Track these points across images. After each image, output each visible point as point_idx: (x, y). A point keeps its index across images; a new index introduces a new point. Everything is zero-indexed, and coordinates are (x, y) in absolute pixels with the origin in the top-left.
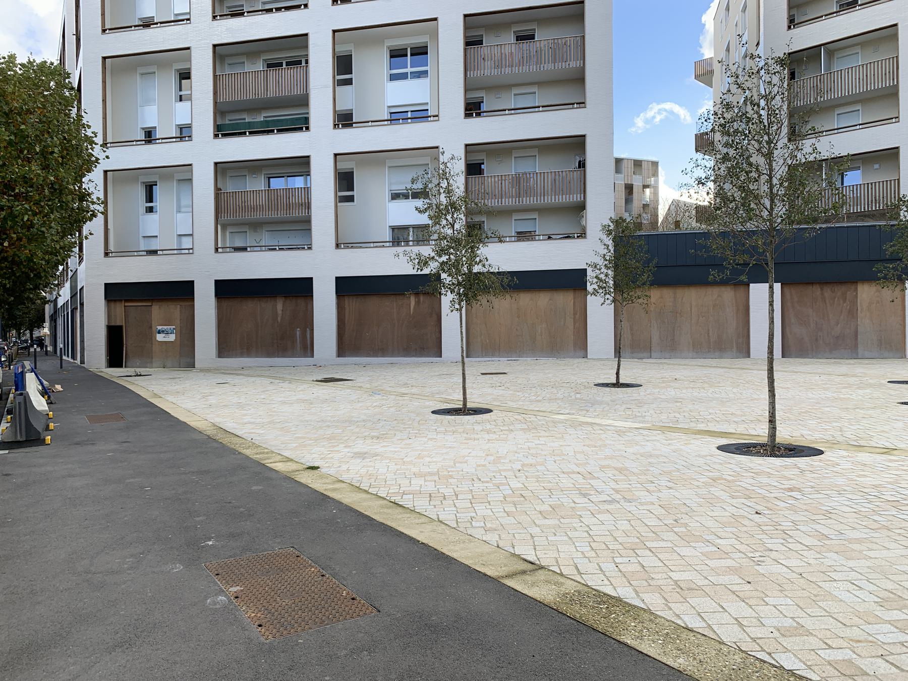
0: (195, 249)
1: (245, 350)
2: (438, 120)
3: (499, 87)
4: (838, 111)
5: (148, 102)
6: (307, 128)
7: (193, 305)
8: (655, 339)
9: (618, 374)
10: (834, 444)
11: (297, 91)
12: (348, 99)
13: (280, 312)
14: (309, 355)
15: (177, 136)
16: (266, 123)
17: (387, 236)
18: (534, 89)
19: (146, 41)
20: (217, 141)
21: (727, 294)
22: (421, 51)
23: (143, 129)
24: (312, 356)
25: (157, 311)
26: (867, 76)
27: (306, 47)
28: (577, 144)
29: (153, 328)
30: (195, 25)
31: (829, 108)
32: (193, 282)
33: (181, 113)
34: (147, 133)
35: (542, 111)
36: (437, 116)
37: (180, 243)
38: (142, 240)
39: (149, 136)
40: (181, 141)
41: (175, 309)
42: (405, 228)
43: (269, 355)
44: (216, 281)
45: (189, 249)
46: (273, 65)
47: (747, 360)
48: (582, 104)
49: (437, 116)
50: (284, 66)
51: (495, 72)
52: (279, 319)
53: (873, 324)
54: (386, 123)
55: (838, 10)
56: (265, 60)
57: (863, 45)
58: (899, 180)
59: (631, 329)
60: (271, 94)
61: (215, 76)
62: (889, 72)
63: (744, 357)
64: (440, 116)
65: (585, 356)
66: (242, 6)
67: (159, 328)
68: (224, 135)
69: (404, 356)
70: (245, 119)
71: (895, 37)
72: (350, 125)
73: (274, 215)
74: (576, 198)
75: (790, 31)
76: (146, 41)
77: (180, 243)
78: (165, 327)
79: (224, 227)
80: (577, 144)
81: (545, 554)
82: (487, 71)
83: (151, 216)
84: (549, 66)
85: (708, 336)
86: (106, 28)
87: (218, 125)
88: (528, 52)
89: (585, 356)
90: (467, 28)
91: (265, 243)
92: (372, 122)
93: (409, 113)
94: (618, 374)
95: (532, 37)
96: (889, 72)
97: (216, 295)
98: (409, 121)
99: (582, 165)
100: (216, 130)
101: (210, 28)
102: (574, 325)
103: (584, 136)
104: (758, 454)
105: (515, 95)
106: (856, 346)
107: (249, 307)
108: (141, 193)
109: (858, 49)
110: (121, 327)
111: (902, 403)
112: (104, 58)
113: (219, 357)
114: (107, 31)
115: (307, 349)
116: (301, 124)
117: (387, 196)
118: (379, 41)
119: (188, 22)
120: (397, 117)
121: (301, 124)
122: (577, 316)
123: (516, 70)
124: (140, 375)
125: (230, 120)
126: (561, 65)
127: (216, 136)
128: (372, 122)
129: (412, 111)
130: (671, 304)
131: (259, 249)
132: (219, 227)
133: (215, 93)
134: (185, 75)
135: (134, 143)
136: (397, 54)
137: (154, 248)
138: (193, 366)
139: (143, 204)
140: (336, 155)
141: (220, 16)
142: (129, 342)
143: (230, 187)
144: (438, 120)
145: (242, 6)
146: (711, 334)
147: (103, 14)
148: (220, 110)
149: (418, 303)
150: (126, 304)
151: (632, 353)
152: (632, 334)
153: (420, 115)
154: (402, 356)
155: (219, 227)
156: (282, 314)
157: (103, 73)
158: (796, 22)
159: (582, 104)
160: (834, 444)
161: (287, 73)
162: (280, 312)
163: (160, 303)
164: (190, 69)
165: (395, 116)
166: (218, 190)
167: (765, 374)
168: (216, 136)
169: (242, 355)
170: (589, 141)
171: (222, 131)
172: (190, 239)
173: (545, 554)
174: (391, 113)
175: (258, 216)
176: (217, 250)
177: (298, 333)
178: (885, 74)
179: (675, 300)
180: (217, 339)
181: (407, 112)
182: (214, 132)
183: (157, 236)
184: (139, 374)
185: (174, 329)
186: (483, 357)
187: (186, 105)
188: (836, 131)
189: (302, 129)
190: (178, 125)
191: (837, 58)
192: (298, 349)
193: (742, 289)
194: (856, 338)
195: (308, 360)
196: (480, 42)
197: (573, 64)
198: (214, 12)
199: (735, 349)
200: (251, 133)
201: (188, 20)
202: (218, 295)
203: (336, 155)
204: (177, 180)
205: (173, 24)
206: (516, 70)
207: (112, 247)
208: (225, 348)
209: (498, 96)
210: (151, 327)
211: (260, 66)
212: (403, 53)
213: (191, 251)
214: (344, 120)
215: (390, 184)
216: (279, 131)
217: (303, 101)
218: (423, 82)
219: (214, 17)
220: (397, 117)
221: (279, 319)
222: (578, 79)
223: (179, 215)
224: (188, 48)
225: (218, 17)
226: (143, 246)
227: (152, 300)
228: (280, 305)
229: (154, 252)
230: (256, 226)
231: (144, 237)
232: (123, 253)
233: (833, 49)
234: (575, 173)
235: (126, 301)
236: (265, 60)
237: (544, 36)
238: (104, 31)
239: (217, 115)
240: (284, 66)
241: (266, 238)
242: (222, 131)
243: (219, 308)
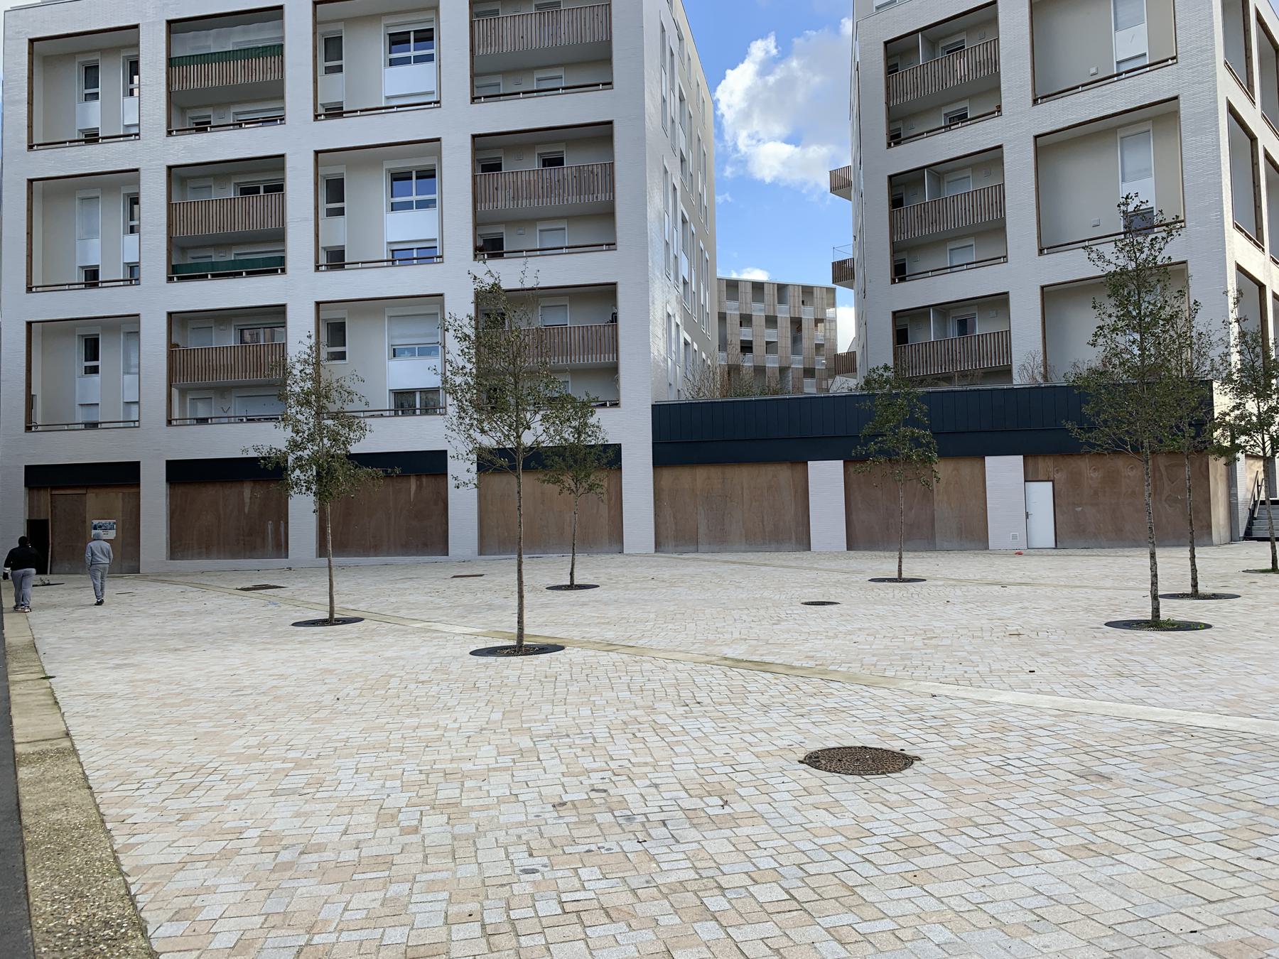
0: (142, 421)
1: (204, 550)
2: (443, 262)
3: (524, 222)
4: (951, 246)
5: (91, 233)
6: (283, 271)
7: (139, 493)
8: (702, 530)
9: (572, 574)
10: (574, 643)
11: (272, 225)
12: (337, 233)
13: (247, 500)
14: (284, 555)
15: (126, 278)
16: (233, 263)
17: (387, 402)
18: (563, 224)
19: (82, 160)
20: (171, 285)
21: (782, 474)
22: (428, 174)
23: (82, 267)
24: (287, 557)
25: (94, 500)
26: (973, 206)
27: (282, 168)
28: (606, 293)
29: (87, 524)
30: (145, 142)
31: (937, 243)
32: (138, 463)
33: (129, 248)
34: (89, 273)
35: (566, 254)
36: (441, 257)
37: (127, 412)
38: (78, 409)
39: (92, 278)
40: (131, 284)
41: (115, 498)
42: (411, 393)
43: (235, 555)
44: (168, 462)
45: (134, 421)
46: (248, 191)
47: (806, 554)
48: (611, 245)
49: (441, 257)
50: (262, 193)
51: (511, 205)
52: (246, 510)
53: (952, 509)
54: (385, 264)
55: (948, 124)
56: (237, 184)
57: (974, 167)
58: (1010, 331)
59: (675, 517)
60: (239, 228)
61: (170, 205)
62: (996, 202)
63: (804, 550)
64: (444, 257)
65: (621, 552)
66: (210, 116)
67: (96, 522)
68: (181, 279)
69: (403, 555)
70: (211, 257)
71: (999, 161)
72: (342, 267)
73: (241, 378)
74: (607, 359)
75: (889, 150)
76: (82, 160)
77: (127, 412)
78: (103, 521)
79: (183, 392)
80: (606, 293)
81: (42, 720)
82: (503, 203)
83: (95, 378)
84: (574, 199)
85: (763, 525)
86: (34, 143)
87: (173, 266)
88: (549, 181)
89: (621, 552)
90: (475, 149)
91: (235, 413)
92: (362, 263)
93: (415, 251)
94: (572, 574)
95: (560, 162)
96: (996, 202)
97: (168, 480)
98: (415, 261)
99: (614, 319)
100: (171, 271)
101: (164, 146)
102: (609, 512)
103: (615, 284)
104: (508, 655)
105: (540, 231)
106: (933, 536)
107: (209, 494)
108: (78, 350)
109: (968, 173)
110: (46, 521)
111: (806, 604)
112: (31, 181)
113: (172, 558)
114: (35, 148)
115: (281, 548)
116: (275, 266)
117: (387, 352)
118: (376, 163)
119: (137, 137)
120: (400, 256)
121: (275, 266)
122: (613, 502)
123: (534, 203)
124: (49, 584)
125: (193, 258)
126: (588, 199)
127: (170, 279)
128: (362, 263)
129: (418, 249)
130: (719, 486)
131: (226, 420)
132: (175, 392)
133: (170, 225)
134: (134, 201)
135: (67, 287)
136: (399, 177)
137: (94, 419)
138: (136, 570)
139: (80, 363)
140: (318, 304)
141: (177, 131)
142: (55, 540)
143: (193, 342)
144: (443, 262)
145: (210, 116)
146: (765, 523)
147: (30, 127)
148: (174, 245)
149: (419, 487)
150: (54, 492)
151: (676, 546)
152: (676, 524)
153: (428, 254)
154: (399, 555)
155: (175, 392)
156: (251, 503)
157: (28, 199)
158: (902, 137)
159: (611, 245)
160: (574, 643)
161: (258, 202)
162: (247, 500)
163: (97, 491)
164: (138, 194)
165: (398, 255)
166: (172, 347)
167: (516, 576)
168: (170, 279)
169: (199, 556)
170: (620, 289)
171: (177, 273)
172: (137, 406)
173: (42, 720)
174: (393, 251)
175: (223, 379)
176: (169, 422)
177: (269, 527)
178: (992, 205)
179: (723, 482)
180: (169, 536)
181: (413, 249)
182: (168, 274)
183: (98, 404)
184: (47, 582)
185: (114, 523)
186: (500, 554)
187: (135, 237)
188: (949, 270)
189: (276, 271)
190: (128, 263)
191: (948, 182)
192: (270, 548)
193: (799, 468)
194: (933, 526)
195: (282, 562)
196: (497, 167)
197: (602, 197)
198: (169, 124)
199: (794, 541)
200: (214, 276)
202: (170, 479)
203: (318, 304)
204: (124, 333)
205: (122, 139)
206: (534, 203)
207: (38, 418)
208: (180, 545)
209: (521, 232)
210: (85, 522)
211: (231, 193)
212: (408, 175)
213: (137, 424)
214: (336, 259)
215: (391, 337)
216: (250, 274)
217: (279, 236)
218: (429, 215)
219: (169, 133)
220: (400, 256)
221: (246, 510)
222: (606, 214)
223: (126, 377)
224: (137, 170)
225: (174, 133)
226: (81, 416)
227: (87, 487)
228: (247, 490)
229: (93, 425)
230: (223, 391)
231: (81, 405)
232: (50, 427)
233: (940, 171)
234: (606, 328)
235: (53, 488)
236: (237, 184)
237: (572, 160)
238: (31, 147)
239: (173, 253)
240: (262, 193)
241: (236, 406)
242: (177, 273)
243: (172, 497)
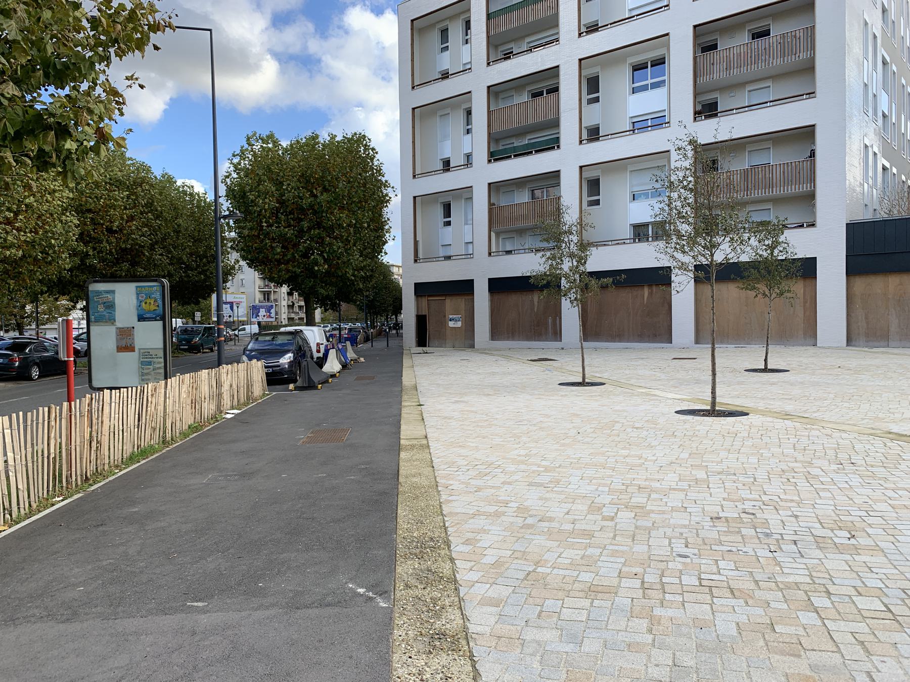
2: (670, 126)
6: (558, 147)
8: (893, 328)
9: (766, 360)
10: (757, 411)
12: (594, 115)
13: (536, 303)
14: (559, 339)
17: (628, 233)
18: (769, 83)
22: (660, 62)
23: (441, 160)
25: (450, 303)
27: (557, 76)
28: (807, 134)
29: (447, 317)
36: (668, 123)
37: (467, 249)
38: (441, 248)
39: (447, 165)
42: (646, 225)
43: (528, 339)
46: (536, 95)
48: (811, 94)
49: (668, 123)
54: (628, 133)
56: (529, 91)
59: (866, 318)
61: (489, 112)
64: (671, 122)
65: (815, 345)
66: (512, 48)
67: (451, 316)
68: (496, 160)
72: (597, 139)
74: (805, 188)
77: (467, 249)
78: (455, 316)
79: (498, 235)
80: (807, 134)
82: (718, 74)
83: (449, 228)
89: (815, 345)
90: (696, 36)
94: (766, 360)
95: (766, 33)
97: (490, 290)
98: (650, 128)
99: (813, 154)
100: (490, 156)
102: (804, 313)
104: (704, 415)
107: (514, 299)
108: (440, 211)
110: (425, 316)
113: (492, 340)
115: (557, 335)
116: (553, 144)
117: (628, 196)
120: (639, 126)
122: (808, 305)
124: (427, 353)
125: (503, 145)
126: (790, 60)
132: (493, 234)
133: (489, 126)
134: (469, 113)
135: (433, 173)
137: (448, 254)
138: (472, 346)
139: (441, 219)
140: (581, 167)
142: (431, 327)
143: (503, 201)
144: (670, 126)
145: (512, 48)
147: (413, 75)
148: (492, 138)
149: (651, 294)
150: (429, 299)
152: (867, 323)
153: (659, 121)
154: (636, 342)
155: (493, 234)
159: (811, 94)
160: (757, 411)
162: (536, 303)
163: (450, 298)
165: (637, 126)
166: (491, 205)
168: (489, 161)
169: (508, 339)
171: (494, 156)
174: (633, 123)
175: (520, 225)
176: (490, 254)
181: (648, 120)
183: (450, 245)
189: (553, 148)
192: (550, 334)
196: (714, 47)
197: (803, 56)
198: (488, 59)
200: (515, 156)
201: (470, 69)
202: (491, 290)
203: (581, 167)
207: (421, 255)
208: (496, 333)
209: (732, 94)
210: (445, 316)
211: (525, 97)
212: (645, 65)
214: (594, 134)
216: (537, 152)
218: (661, 92)
220: (639, 126)
222: (808, 69)
223: (466, 226)
225: (491, 64)
226: (442, 252)
227: (446, 295)
229: (448, 258)
230: (521, 232)
231: (443, 245)
232: (428, 259)
234: (804, 163)
235: (429, 296)
236: (529, 91)
239: (491, 144)
240: (545, 95)
242: (494, 156)
243: (492, 301)
